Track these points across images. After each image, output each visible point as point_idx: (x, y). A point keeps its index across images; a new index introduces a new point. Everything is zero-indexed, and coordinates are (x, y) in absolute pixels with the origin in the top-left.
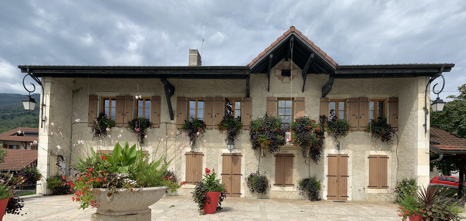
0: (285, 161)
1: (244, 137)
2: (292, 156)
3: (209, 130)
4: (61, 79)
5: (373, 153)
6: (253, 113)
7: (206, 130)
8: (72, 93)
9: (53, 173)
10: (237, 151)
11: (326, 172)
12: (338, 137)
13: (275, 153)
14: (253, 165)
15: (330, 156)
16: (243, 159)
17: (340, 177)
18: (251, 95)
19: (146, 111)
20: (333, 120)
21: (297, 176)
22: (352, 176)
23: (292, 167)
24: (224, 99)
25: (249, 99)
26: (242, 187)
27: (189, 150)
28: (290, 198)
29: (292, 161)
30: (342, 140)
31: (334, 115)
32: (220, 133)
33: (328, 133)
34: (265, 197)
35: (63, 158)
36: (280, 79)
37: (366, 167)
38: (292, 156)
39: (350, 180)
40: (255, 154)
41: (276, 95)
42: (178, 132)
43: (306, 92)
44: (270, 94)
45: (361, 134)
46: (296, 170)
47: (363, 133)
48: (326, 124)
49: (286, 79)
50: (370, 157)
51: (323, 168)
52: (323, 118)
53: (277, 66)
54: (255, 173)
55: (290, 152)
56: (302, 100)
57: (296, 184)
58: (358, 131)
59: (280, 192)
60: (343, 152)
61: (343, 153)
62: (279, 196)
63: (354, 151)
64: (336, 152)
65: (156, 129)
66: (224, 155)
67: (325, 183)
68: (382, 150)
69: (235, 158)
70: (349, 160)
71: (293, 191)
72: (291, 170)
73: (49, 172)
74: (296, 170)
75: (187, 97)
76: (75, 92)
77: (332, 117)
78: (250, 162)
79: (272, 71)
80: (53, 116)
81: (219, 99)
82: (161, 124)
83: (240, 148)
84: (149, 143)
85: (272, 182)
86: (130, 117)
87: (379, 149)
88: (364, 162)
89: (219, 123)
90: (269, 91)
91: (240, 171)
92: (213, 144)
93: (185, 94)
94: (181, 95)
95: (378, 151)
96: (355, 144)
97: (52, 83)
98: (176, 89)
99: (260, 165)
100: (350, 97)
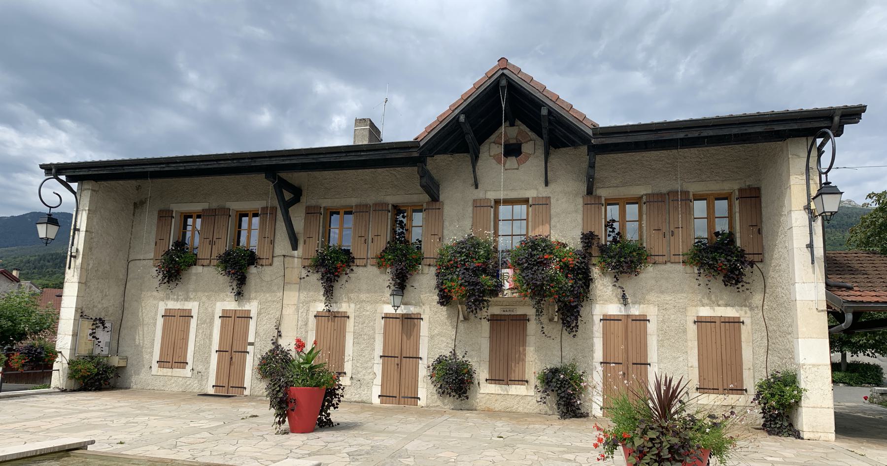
0: (508, 330)
1: (425, 282)
4: (113, 183)
5: (705, 312)
6: (446, 232)
7: (354, 268)
8: (132, 207)
9: (84, 350)
10: (412, 310)
11: (598, 354)
12: (623, 279)
13: (484, 313)
14: (444, 339)
15: (606, 319)
16: (424, 326)
18: (441, 198)
19: (252, 236)
20: (615, 240)
23: (524, 343)
24: (390, 207)
25: (437, 205)
26: (420, 384)
27: (321, 307)
28: (520, 409)
29: (524, 329)
30: (630, 284)
31: (617, 231)
32: (381, 273)
33: (602, 269)
34: (467, 407)
35: (103, 323)
36: (499, 162)
37: (689, 344)
40: (449, 316)
41: (492, 195)
42: (304, 273)
43: (552, 186)
44: (479, 194)
45: (680, 273)
46: (532, 349)
47: (680, 267)
48: (595, 251)
49: (512, 161)
50: (699, 321)
52: (588, 238)
53: (493, 137)
54: (448, 354)
55: (520, 311)
56: (545, 203)
57: (534, 380)
58: (669, 265)
59: (498, 397)
60: (635, 311)
61: (637, 313)
62: (498, 406)
63: (661, 307)
64: (620, 311)
66: (386, 317)
67: (596, 378)
68: (726, 305)
69: (409, 322)
70: (651, 327)
71: (525, 395)
72: (521, 349)
73: (74, 349)
74: (532, 349)
75: (323, 205)
76: (138, 205)
77: (613, 234)
78: (438, 333)
79: (484, 148)
80: (91, 249)
81: (380, 207)
82: (275, 259)
83: (419, 304)
84: (253, 295)
85: (482, 373)
86: (221, 248)
87: (721, 302)
88: (685, 331)
89: (379, 253)
90: (477, 187)
91: (417, 350)
92: (368, 295)
93: (320, 201)
94: (313, 202)
95: (717, 308)
96: (662, 292)
97: (92, 190)
98: (304, 193)
99: (458, 338)
100: (649, 192)
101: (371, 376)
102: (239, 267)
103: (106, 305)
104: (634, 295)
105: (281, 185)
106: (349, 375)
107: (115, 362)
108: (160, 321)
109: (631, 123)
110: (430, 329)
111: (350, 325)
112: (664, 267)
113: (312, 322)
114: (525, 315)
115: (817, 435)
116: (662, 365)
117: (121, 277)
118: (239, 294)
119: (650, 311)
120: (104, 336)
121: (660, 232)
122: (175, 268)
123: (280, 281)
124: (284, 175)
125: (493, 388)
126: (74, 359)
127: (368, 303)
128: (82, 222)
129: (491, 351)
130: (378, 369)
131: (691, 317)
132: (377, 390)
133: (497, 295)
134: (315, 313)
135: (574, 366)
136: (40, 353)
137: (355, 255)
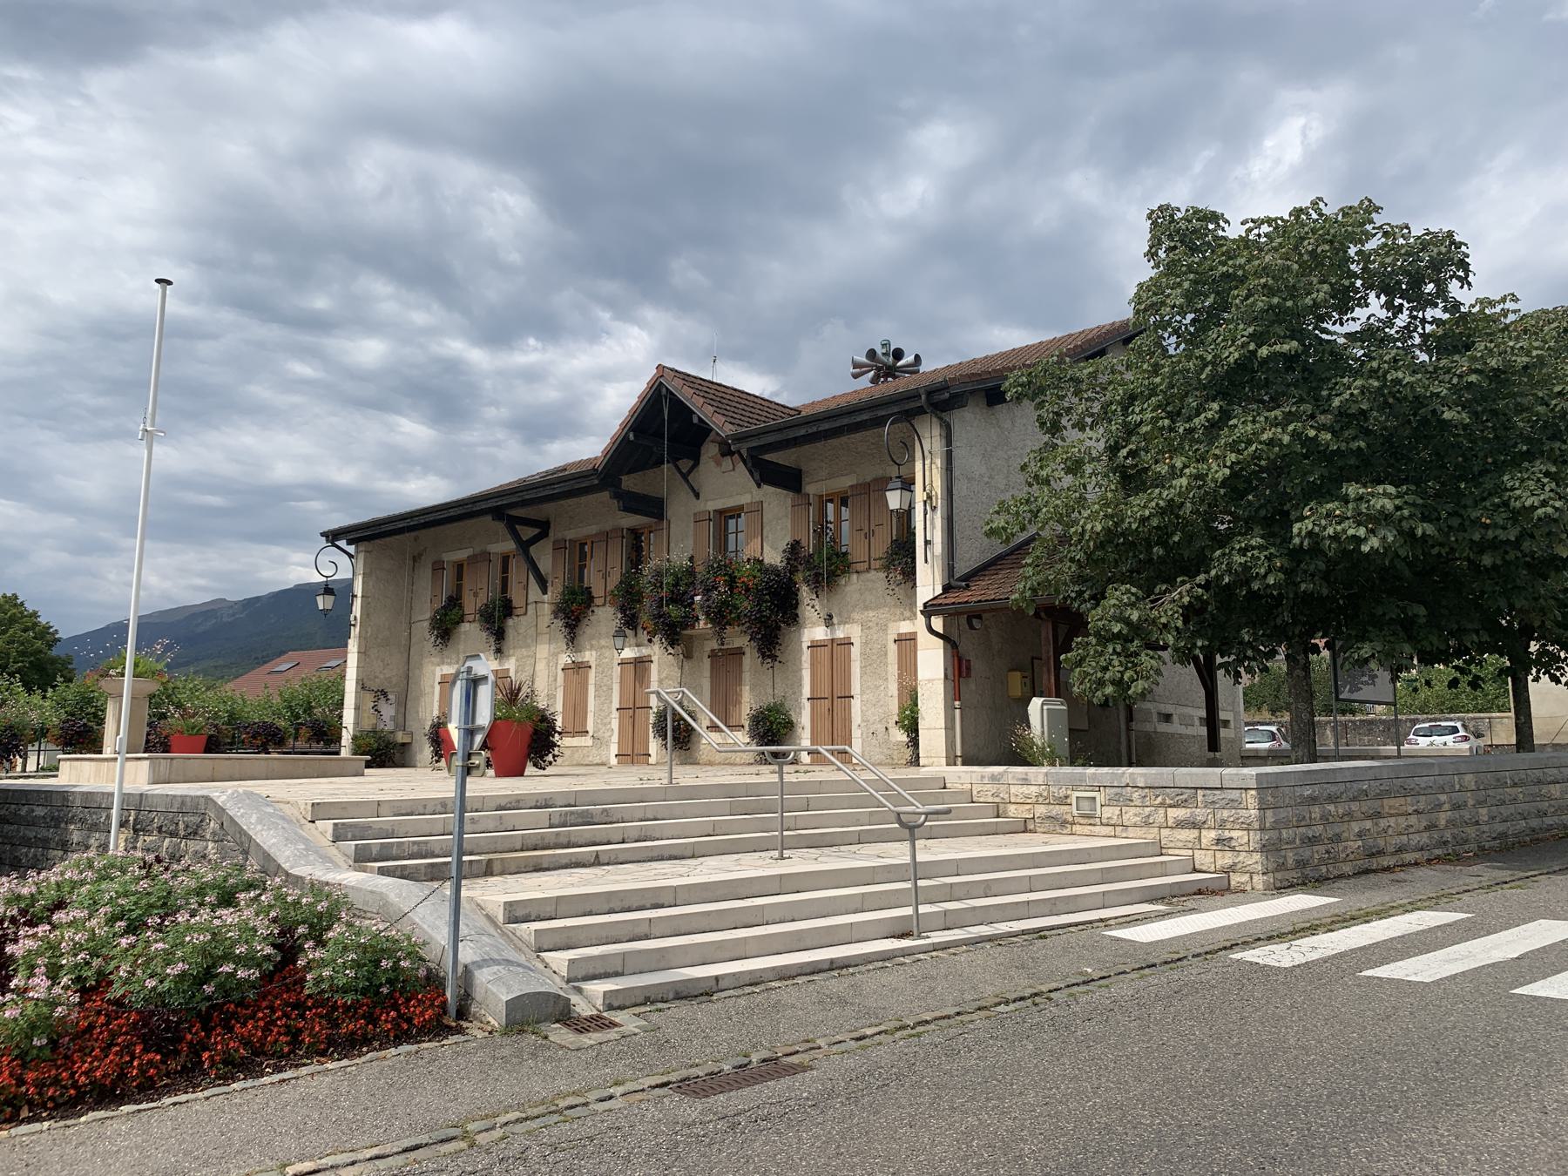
2: (739, 652)
8: (409, 562)
9: (367, 725)
11: (806, 691)
15: (814, 646)
21: (748, 703)
23: (740, 682)
27: (565, 659)
29: (741, 665)
36: (718, 464)
38: (739, 652)
39: (856, 705)
49: (727, 462)
51: (800, 679)
52: (795, 547)
56: (758, 508)
57: (747, 724)
58: (873, 572)
63: (865, 626)
70: (855, 651)
73: (356, 723)
94: (559, 536)
96: (866, 608)
103: (388, 675)
104: (840, 615)
105: (512, 524)
107: (400, 737)
108: (437, 688)
111: (592, 674)
113: (560, 674)
118: (499, 651)
119: (851, 631)
120: (388, 711)
122: (445, 629)
124: (513, 512)
125: (715, 737)
127: (607, 653)
128: (358, 589)
130: (615, 724)
131: (892, 636)
132: (614, 749)
135: (782, 705)
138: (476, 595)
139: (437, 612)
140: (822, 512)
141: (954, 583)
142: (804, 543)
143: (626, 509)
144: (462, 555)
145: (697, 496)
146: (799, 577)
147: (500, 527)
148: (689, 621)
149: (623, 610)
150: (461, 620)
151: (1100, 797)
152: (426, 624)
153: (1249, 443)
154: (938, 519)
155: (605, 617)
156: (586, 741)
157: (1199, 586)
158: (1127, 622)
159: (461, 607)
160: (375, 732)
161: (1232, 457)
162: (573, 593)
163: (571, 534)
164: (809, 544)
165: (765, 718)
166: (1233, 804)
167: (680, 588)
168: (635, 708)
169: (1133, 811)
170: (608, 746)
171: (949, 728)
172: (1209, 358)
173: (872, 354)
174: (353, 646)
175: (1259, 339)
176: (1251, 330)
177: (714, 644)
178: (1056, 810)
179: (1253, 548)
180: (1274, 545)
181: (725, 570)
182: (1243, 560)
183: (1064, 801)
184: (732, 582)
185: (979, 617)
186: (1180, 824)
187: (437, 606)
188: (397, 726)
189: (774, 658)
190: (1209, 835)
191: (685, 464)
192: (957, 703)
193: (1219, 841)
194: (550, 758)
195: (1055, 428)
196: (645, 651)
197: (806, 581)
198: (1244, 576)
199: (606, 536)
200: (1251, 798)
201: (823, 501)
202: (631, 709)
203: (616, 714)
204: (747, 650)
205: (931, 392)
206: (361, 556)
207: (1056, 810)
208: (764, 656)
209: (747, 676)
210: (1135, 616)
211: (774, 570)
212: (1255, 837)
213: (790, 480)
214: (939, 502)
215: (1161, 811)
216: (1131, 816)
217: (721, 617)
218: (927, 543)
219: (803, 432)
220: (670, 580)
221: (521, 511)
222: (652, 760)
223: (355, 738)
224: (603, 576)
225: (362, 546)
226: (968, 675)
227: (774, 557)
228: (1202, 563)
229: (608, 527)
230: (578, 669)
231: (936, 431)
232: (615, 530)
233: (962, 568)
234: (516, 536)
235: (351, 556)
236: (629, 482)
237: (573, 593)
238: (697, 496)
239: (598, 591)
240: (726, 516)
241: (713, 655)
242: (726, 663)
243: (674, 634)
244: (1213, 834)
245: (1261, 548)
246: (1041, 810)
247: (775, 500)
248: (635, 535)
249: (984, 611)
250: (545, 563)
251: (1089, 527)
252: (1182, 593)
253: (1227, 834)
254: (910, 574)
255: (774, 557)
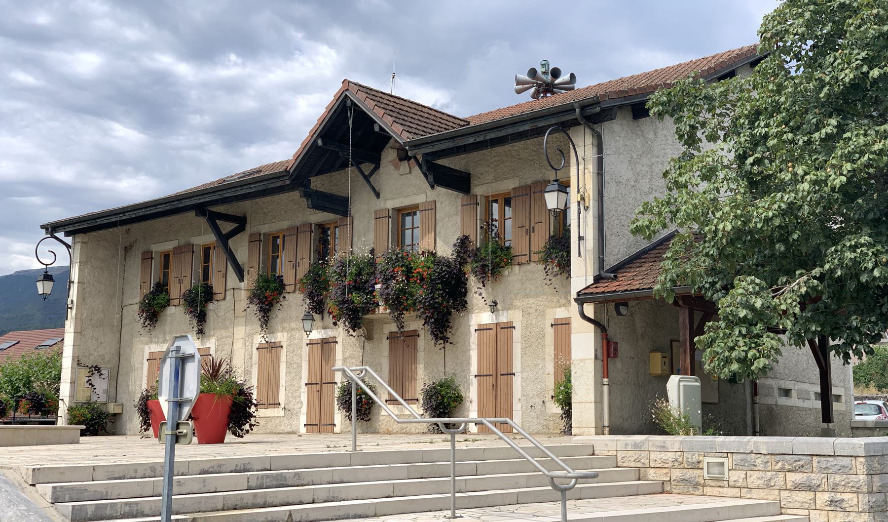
2: (415, 335)
3: (291, 295)
4: (102, 232)
7: (286, 295)
8: (121, 252)
9: (82, 398)
11: (474, 369)
14: (354, 361)
15: (480, 329)
17: (498, 376)
22: (522, 373)
23: (414, 360)
27: (259, 340)
34: (372, 430)
36: (397, 167)
37: (547, 349)
38: (415, 335)
39: (517, 381)
41: (392, 204)
46: (422, 366)
49: (404, 166)
52: (464, 242)
56: (432, 207)
57: (421, 398)
58: (533, 264)
60: (504, 318)
61: (505, 321)
63: (525, 312)
65: (220, 303)
70: (517, 334)
73: (72, 396)
75: (263, 232)
76: (127, 249)
80: (84, 299)
82: (228, 293)
84: (212, 332)
88: (544, 337)
93: (260, 227)
94: (255, 230)
98: (248, 221)
100: (517, 185)
101: (299, 405)
102: (200, 304)
103: (101, 352)
105: (213, 219)
106: (282, 406)
107: (112, 409)
109: (694, 59)
110: (343, 351)
111: (284, 353)
112: (527, 267)
113: (255, 353)
114: (416, 331)
115: (582, 430)
116: (525, 374)
117: (115, 323)
118: (201, 332)
119: (514, 316)
120: (101, 385)
121: (524, 229)
122: (153, 311)
123: (230, 315)
124: (214, 209)
125: (392, 409)
126: (74, 406)
127: (297, 333)
128: (75, 275)
129: (390, 370)
130: (304, 398)
132: (303, 420)
133: (374, 312)
134: (257, 346)
135: (452, 381)
136: (41, 399)
137: (286, 282)
138: (181, 282)
139: (146, 296)
140: (489, 211)
141: (604, 274)
142: (472, 238)
143: (316, 207)
144: (168, 246)
145: (378, 195)
146: (468, 268)
147: (202, 222)
148: (370, 307)
149: (311, 296)
150: (168, 304)
151: (728, 462)
152: (136, 308)
153: (862, 153)
154: (590, 218)
155: (295, 303)
156: (278, 412)
157: (815, 278)
158: (752, 308)
159: (167, 292)
160: (89, 404)
161: (848, 166)
162: (267, 281)
163: (265, 229)
164: (477, 240)
165: (438, 393)
166: (843, 470)
167: (361, 278)
168: (321, 383)
169: (756, 474)
170: (298, 417)
171: (598, 402)
172: (827, 79)
173: (533, 73)
174: (70, 326)
175: (871, 62)
176: (863, 54)
177: (393, 327)
178: (690, 474)
179: (862, 245)
180: (880, 242)
181: (403, 263)
182: (853, 255)
183: (696, 466)
184: (408, 272)
185: (626, 304)
186: (798, 488)
187: (146, 291)
188: (109, 397)
189: (445, 339)
190: (823, 498)
191: (367, 167)
192: (605, 380)
193: (832, 502)
194: (247, 427)
195: (691, 140)
196: (330, 333)
197: (475, 273)
198: (855, 270)
199: (296, 231)
200: (860, 465)
201: (490, 201)
202: (319, 384)
203: (304, 389)
204: (422, 333)
205: (583, 108)
206: (78, 247)
207: (690, 474)
208: (437, 338)
209: (421, 355)
210: (758, 304)
211: (446, 263)
212: (864, 499)
213: (460, 182)
214: (591, 202)
215: (781, 475)
216: (754, 478)
217: (399, 303)
218: (580, 238)
219: (471, 140)
220: (353, 270)
221: (220, 208)
222: (337, 429)
223: (70, 409)
224: (294, 266)
225: (80, 238)
226: (616, 356)
227: (446, 250)
228: (817, 258)
229: (298, 223)
230: (272, 348)
231: (589, 140)
232: (304, 225)
233: (611, 261)
234: (217, 230)
235: (68, 246)
236: (318, 183)
237: (267, 281)
238: (378, 195)
239: (288, 279)
240: (404, 213)
241: (392, 337)
242: (403, 341)
243: (356, 317)
244: (827, 496)
245: (870, 245)
246: (676, 474)
247: (447, 201)
248: (323, 229)
249: (629, 299)
250: (242, 254)
251: (721, 226)
252: (800, 284)
253: (839, 496)
254: (565, 266)
255: (446, 250)
